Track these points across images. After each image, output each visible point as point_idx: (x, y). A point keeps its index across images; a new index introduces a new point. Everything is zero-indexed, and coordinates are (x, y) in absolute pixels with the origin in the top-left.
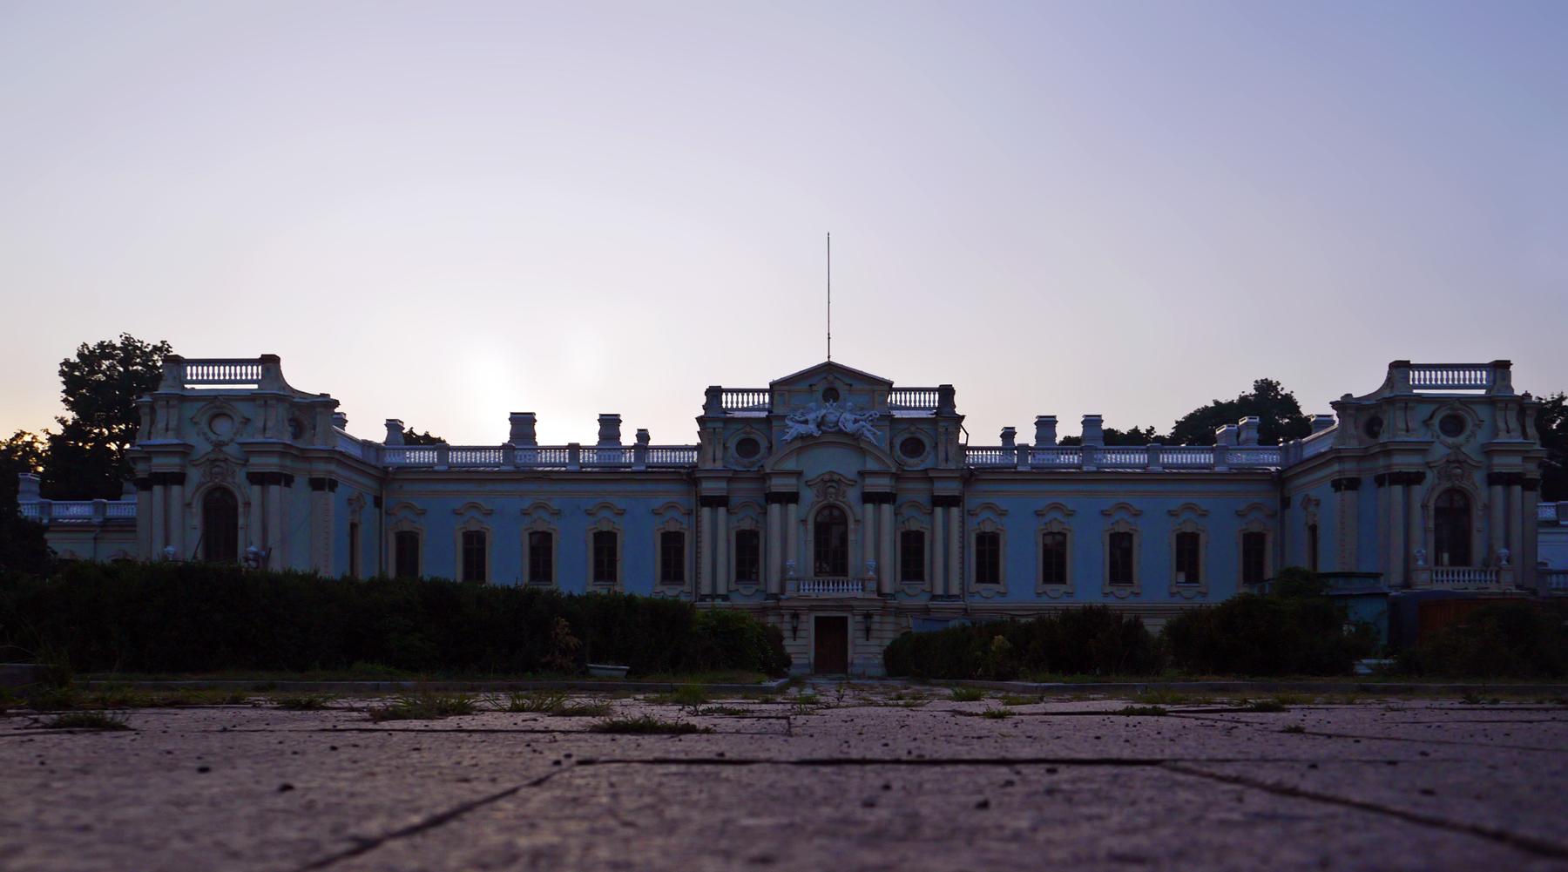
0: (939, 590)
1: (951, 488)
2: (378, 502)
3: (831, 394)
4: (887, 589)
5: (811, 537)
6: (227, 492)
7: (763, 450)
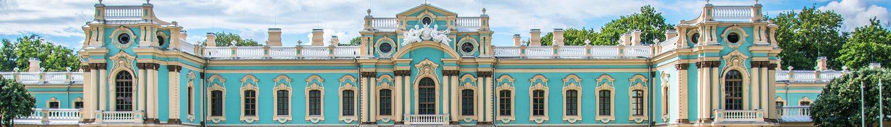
0: (481, 120)
2: (202, 75)
3: (427, 20)
4: (455, 119)
5: (416, 93)
6: (127, 72)
7: (393, 49)
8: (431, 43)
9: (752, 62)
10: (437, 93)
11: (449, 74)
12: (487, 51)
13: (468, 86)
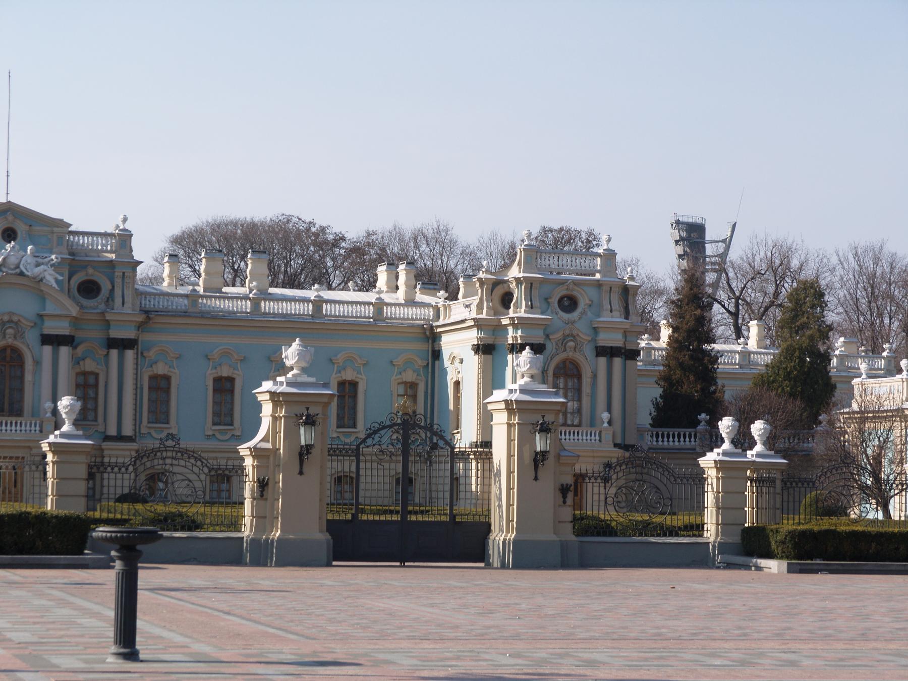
0: (113, 432)
1: (129, 333)
8: (20, 280)
9: (596, 347)
10: (28, 377)
11: (53, 341)
12: (128, 299)
13: (89, 365)
